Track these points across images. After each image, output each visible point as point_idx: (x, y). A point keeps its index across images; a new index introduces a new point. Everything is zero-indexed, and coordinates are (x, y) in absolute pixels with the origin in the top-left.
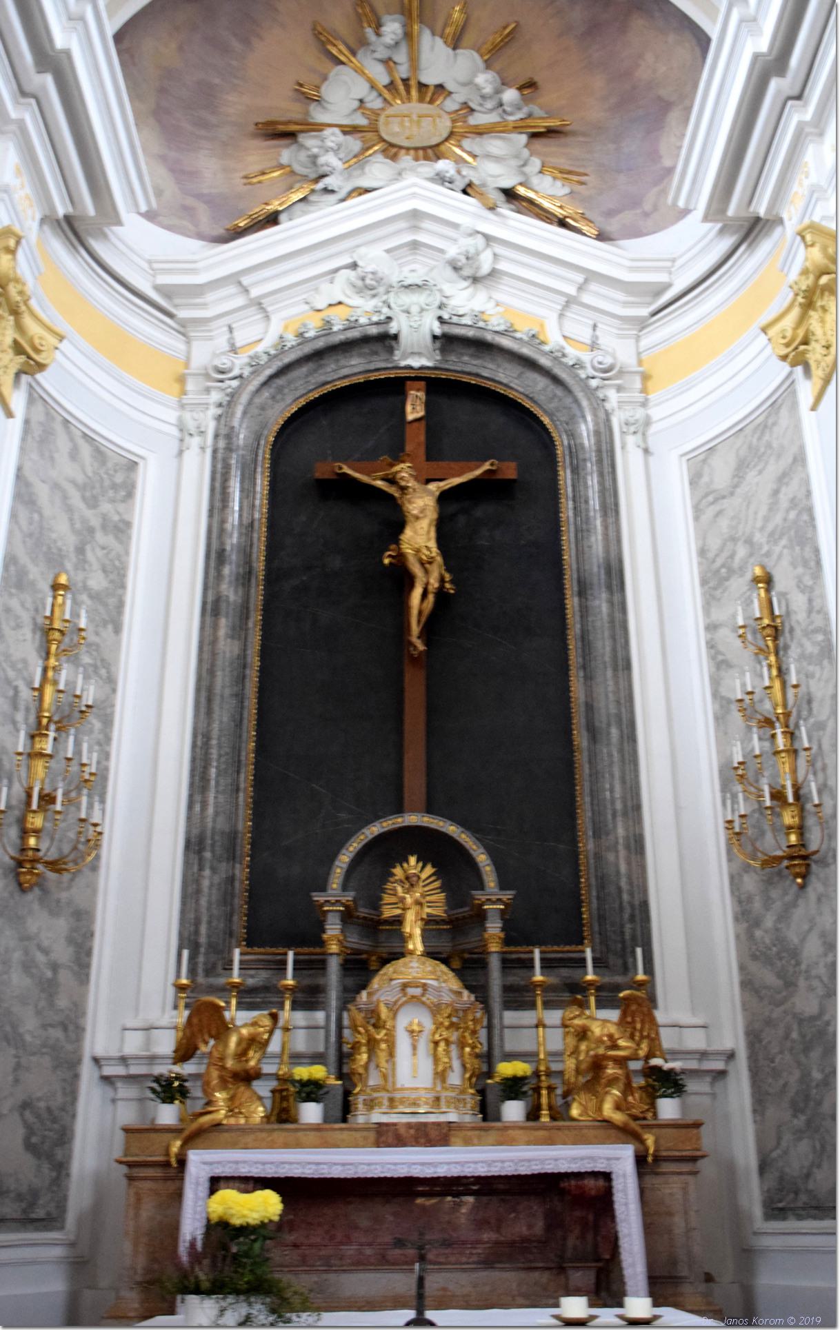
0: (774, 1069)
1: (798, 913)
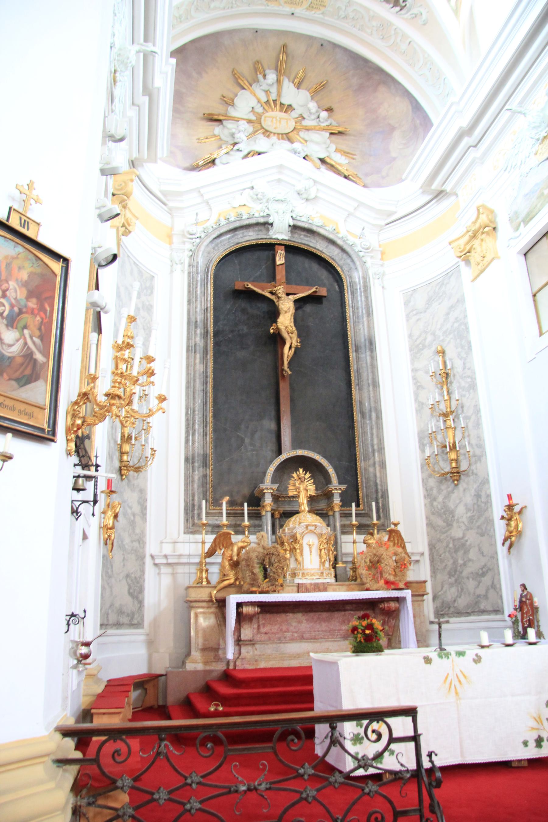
0: (441, 559)
1: (454, 496)
